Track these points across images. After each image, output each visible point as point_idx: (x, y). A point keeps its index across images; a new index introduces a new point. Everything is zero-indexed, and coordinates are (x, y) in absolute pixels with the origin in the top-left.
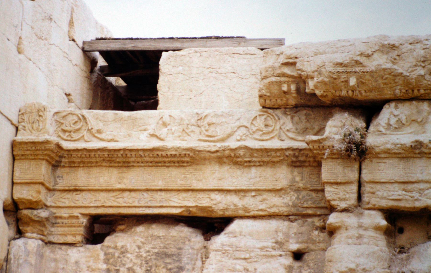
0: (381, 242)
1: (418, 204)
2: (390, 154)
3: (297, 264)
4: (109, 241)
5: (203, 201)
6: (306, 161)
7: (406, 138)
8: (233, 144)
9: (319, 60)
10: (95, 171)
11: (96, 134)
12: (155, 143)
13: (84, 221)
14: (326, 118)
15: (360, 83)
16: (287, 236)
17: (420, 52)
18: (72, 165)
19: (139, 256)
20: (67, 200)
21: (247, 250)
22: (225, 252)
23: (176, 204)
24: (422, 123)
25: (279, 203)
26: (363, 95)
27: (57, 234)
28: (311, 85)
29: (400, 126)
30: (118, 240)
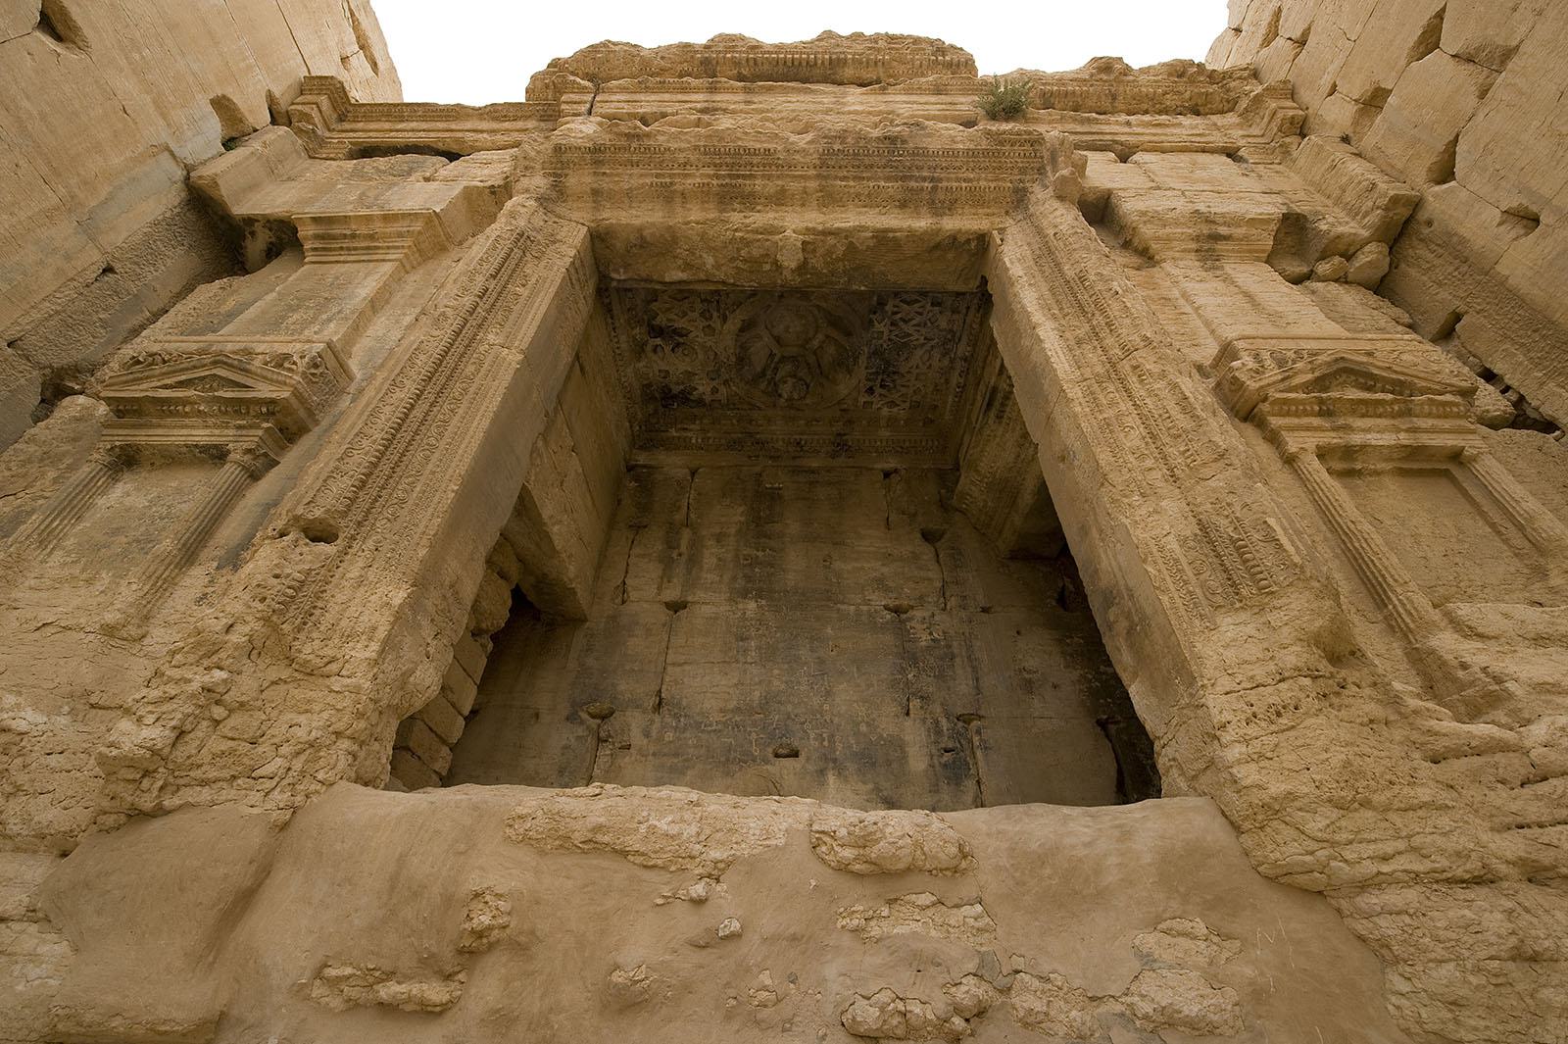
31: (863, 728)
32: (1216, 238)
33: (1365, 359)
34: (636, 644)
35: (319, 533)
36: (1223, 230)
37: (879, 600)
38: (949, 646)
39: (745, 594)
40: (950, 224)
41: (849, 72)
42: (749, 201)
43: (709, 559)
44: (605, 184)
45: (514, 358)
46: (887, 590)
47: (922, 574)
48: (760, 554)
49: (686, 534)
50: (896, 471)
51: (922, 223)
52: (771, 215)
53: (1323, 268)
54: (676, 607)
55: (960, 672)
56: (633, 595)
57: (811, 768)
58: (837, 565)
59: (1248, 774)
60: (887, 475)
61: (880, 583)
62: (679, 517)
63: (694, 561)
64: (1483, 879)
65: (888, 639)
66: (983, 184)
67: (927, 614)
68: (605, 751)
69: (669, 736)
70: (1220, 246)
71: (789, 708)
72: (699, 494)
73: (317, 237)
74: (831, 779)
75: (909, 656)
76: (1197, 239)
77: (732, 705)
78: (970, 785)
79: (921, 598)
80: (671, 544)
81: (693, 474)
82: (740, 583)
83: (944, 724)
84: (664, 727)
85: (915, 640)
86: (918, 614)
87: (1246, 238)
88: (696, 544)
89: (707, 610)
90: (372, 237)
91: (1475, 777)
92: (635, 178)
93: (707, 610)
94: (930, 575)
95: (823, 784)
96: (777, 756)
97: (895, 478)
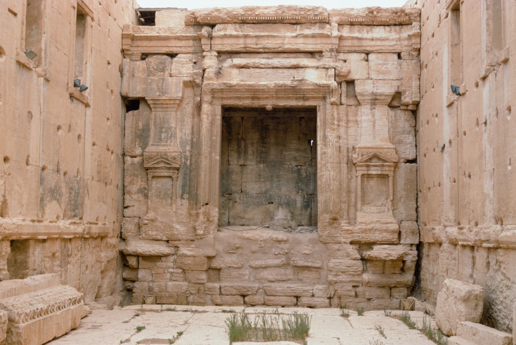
0: (216, 59)
1: (225, 50)
2: (218, 37)
3: (195, 65)
4: (147, 60)
5: (171, 49)
6: (198, 39)
7: (222, 33)
8: (178, 35)
9: (200, 13)
10: (143, 42)
11: (143, 32)
12: (158, 35)
13: (140, 54)
14: (202, 28)
15: (211, 19)
16: (192, 58)
18: (137, 40)
19: (155, 63)
20: (136, 49)
21: (182, 62)
22: (177, 62)
23: (164, 50)
24: (225, 29)
25: (190, 50)
26: (212, 22)
27: (134, 58)
28: (198, 19)
29: (220, 30)
30: (149, 59)
31: (288, 197)
32: (376, 99)
33: (379, 154)
34: (234, 177)
35: (207, 204)
36: (378, 97)
37: (294, 164)
38: (310, 177)
40: (308, 103)
42: (258, 98)
43: (250, 152)
44: (225, 96)
45: (218, 158)
46: (296, 161)
47: (307, 155)
48: (263, 149)
49: (243, 143)
50: (303, 117)
51: (300, 103)
52: (264, 101)
53: (402, 107)
55: (311, 183)
56: (231, 163)
57: (276, 206)
58: (284, 153)
59: (319, 232)
60: (300, 118)
61: (295, 159)
62: (240, 136)
63: (246, 152)
64: (340, 243)
65: (295, 175)
66: (316, 95)
67: (306, 168)
68: (231, 202)
69: (245, 199)
71: (271, 193)
72: (245, 128)
73: (153, 104)
74: (280, 208)
75: (299, 179)
76: (371, 100)
77: (258, 192)
78: (309, 209)
79: (305, 163)
80: (239, 147)
81: (242, 118)
82: (258, 159)
84: (243, 197)
85: (302, 175)
86: (304, 168)
87: (384, 99)
88: (246, 147)
90: (167, 104)
91: (344, 233)
92: (231, 95)
93: (250, 167)
94: (309, 156)
95: (278, 209)
96: (269, 203)
97: (303, 121)
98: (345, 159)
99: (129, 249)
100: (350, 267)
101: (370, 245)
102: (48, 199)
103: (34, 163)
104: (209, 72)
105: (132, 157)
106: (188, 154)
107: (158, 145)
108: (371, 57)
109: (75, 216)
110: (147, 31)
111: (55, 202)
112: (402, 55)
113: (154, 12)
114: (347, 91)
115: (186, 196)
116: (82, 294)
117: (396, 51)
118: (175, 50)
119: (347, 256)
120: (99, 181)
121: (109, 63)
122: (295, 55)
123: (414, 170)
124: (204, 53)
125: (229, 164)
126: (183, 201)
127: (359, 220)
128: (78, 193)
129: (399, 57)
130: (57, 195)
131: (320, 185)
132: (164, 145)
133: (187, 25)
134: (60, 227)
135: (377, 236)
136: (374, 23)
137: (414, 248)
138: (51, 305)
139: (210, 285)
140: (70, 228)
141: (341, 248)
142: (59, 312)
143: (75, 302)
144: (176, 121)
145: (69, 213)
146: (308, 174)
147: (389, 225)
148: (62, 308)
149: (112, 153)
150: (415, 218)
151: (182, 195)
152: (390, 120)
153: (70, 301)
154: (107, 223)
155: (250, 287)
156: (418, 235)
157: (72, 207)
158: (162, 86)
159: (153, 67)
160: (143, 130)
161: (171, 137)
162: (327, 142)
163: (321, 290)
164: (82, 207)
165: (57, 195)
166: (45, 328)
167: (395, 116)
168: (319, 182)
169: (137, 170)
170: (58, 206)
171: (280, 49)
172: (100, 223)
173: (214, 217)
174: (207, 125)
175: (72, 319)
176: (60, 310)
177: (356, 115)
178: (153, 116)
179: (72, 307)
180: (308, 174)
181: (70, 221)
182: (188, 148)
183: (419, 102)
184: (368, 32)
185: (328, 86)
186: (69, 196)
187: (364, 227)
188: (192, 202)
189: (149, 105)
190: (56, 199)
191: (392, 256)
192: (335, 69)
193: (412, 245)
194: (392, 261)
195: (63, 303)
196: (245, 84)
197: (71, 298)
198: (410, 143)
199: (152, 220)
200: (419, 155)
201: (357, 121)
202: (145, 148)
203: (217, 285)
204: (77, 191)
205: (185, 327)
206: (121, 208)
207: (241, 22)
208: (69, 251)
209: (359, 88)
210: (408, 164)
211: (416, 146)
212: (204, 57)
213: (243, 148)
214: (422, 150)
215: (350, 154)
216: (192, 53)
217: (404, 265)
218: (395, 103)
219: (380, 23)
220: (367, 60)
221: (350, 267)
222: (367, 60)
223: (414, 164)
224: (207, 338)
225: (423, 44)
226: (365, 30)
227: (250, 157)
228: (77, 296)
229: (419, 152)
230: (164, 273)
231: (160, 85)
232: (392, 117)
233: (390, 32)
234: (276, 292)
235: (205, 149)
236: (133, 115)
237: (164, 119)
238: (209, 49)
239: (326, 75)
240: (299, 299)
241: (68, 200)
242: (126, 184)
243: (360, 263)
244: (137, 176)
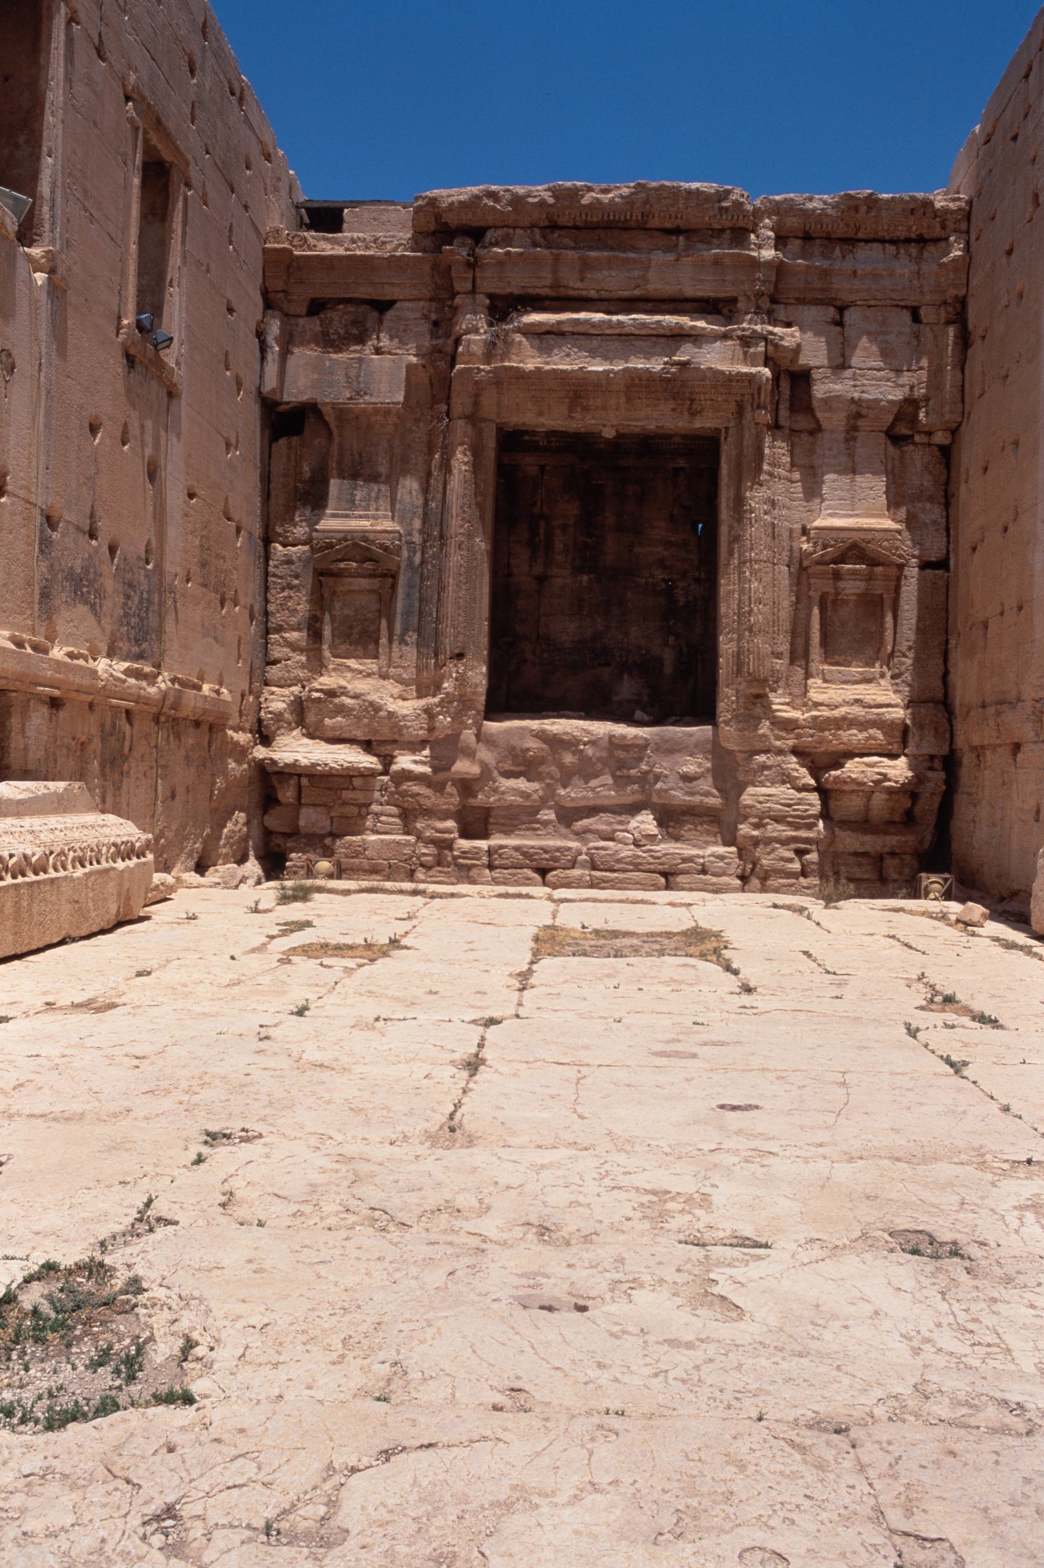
16: (429, 311)
17: (508, 196)
23: (364, 292)
33: (864, 545)
36: (864, 412)
37: (659, 575)
39: (578, 570)
40: (698, 424)
41: (655, 223)
42: (586, 409)
43: (559, 546)
49: (542, 524)
50: (682, 469)
54: (542, 579)
60: (677, 471)
61: (661, 563)
69: (545, 655)
70: (860, 423)
74: (625, 677)
81: (542, 468)
83: (685, 649)
86: (681, 584)
89: (559, 581)
93: (559, 581)
96: (600, 665)
98: (785, 554)
99: (276, 756)
100: (789, 806)
101: (838, 760)
102: (64, 596)
103: (22, 493)
104: (469, 340)
105: (284, 546)
106: (417, 538)
107: (347, 516)
108: (852, 316)
109: (140, 657)
110: (324, 246)
111: (83, 609)
112: (922, 312)
113: (341, 210)
114: (792, 396)
115: (412, 637)
116: (150, 836)
117: (908, 303)
118: (388, 293)
119: (784, 782)
120: (205, 585)
121: (230, 310)
122: (672, 306)
123: (941, 583)
124: (458, 300)
125: (510, 575)
126: (404, 648)
127: (814, 695)
128: (148, 600)
129: (916, 318)
130: (89, 592)
131: (727, 616)
132: (361, 517)
133: (420, 236)
134: (96, 672)
135: (854, 736)
136: (860, 235)
137: (937, 764)
138: (57, 850)
139: (464, 844)
140: (124, 681)
141: (769, 763)
142: (80, 872)
143: (127, 851)
144: (391, 461)
145: (124, 646)
146: (691, 598)
147: (884, 710)
148: (91, 864)
149: (238, 530)
150: (940, 695)
151: (403, 634)
152: (890, 466)
153: (113, 849)
154: (224, 690)
155: (558, 849)
156: (948, 735)
157: (133, 632)
158: (358, 376)
159: (338, 334)
160: (312, 481)
161: (377, 498)
162: (745, 512)
163: (721, 858)
164: (160, 640)
165: (89, 592)
166: (35, 908)
167: (902, 458)
168: (723, 609)
169: (297, 577)
170: (91, 619)
171: (637, 292)
172: (206, 687)
173: (477, 686)
174: (464, 468)
175: (119, 895)
176: (83, 866)
177: (811, 452)
178: (335, 450)
179: (120, 865)
180: (691, 598)
181: (126, 665)
182: (417, 524)
183: (960, 424)
184: (844, 257)
185: (750, 378)
186: (125, 604)
187: (826, 713)
188: (424, 650)
189: (326, 424)
190: (86, 603)
191: (890, 780)
192: (766, 339)
193: (932, 757)
194: (890, 791)
195: (92, 850)
196: (554, 370)
197: (119, 841)
198: (934, 522)
199: (331, 693)
200: (956, 550)
201: (812, 467)
202: (317, 523)
203: (483, 844)
204: (145, 596)
205: (407, 925)
206: (258, 663)
207: (547, 223)
208: (124, 738)
209: (820, 390)
210: (928, 571)
211: (948, 530)
212: (455, 310)
213: (542, 536)
214: (967, 533)
215: (795, 544)
216: (431, 300)
217: (913, 804)
218: (903, 430)
219: (872, 236)
220: (840, 323)
221: (789, 806)
222: (840, 323)
223: (941, 572)
224: (470, 946)
225: (974, 282)
226: (837, 252)
227: (559, 558)
228: (134, 839)
229: (957, 541)
230: (359, 815)
231: (352, 373)
232: (893, 459)
233: (896, 257)
234: (619, 861)
235: (456, 526)
236: (290, 448)
237: (360, 455)
238: (469, 286)
239: (745, 353)
240: (671, 878)
241: (121, 612)
242: (271, 608)
243: (814, 798)
244: (298, 591)
